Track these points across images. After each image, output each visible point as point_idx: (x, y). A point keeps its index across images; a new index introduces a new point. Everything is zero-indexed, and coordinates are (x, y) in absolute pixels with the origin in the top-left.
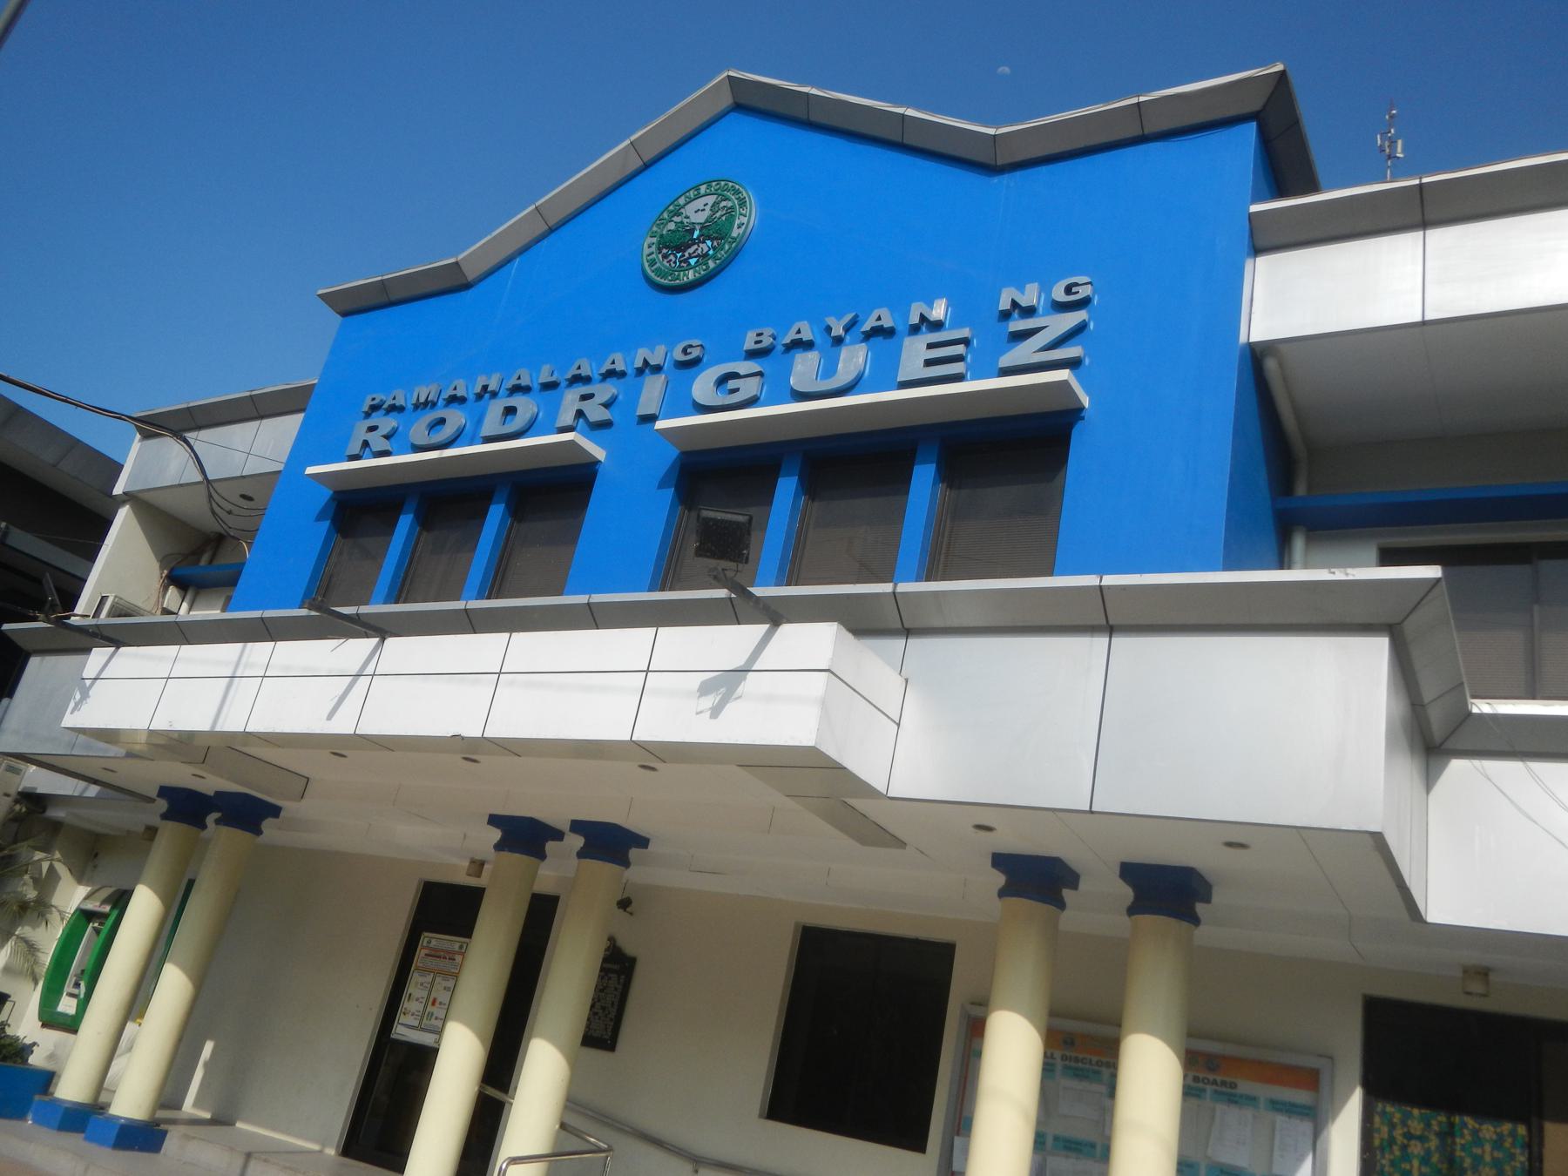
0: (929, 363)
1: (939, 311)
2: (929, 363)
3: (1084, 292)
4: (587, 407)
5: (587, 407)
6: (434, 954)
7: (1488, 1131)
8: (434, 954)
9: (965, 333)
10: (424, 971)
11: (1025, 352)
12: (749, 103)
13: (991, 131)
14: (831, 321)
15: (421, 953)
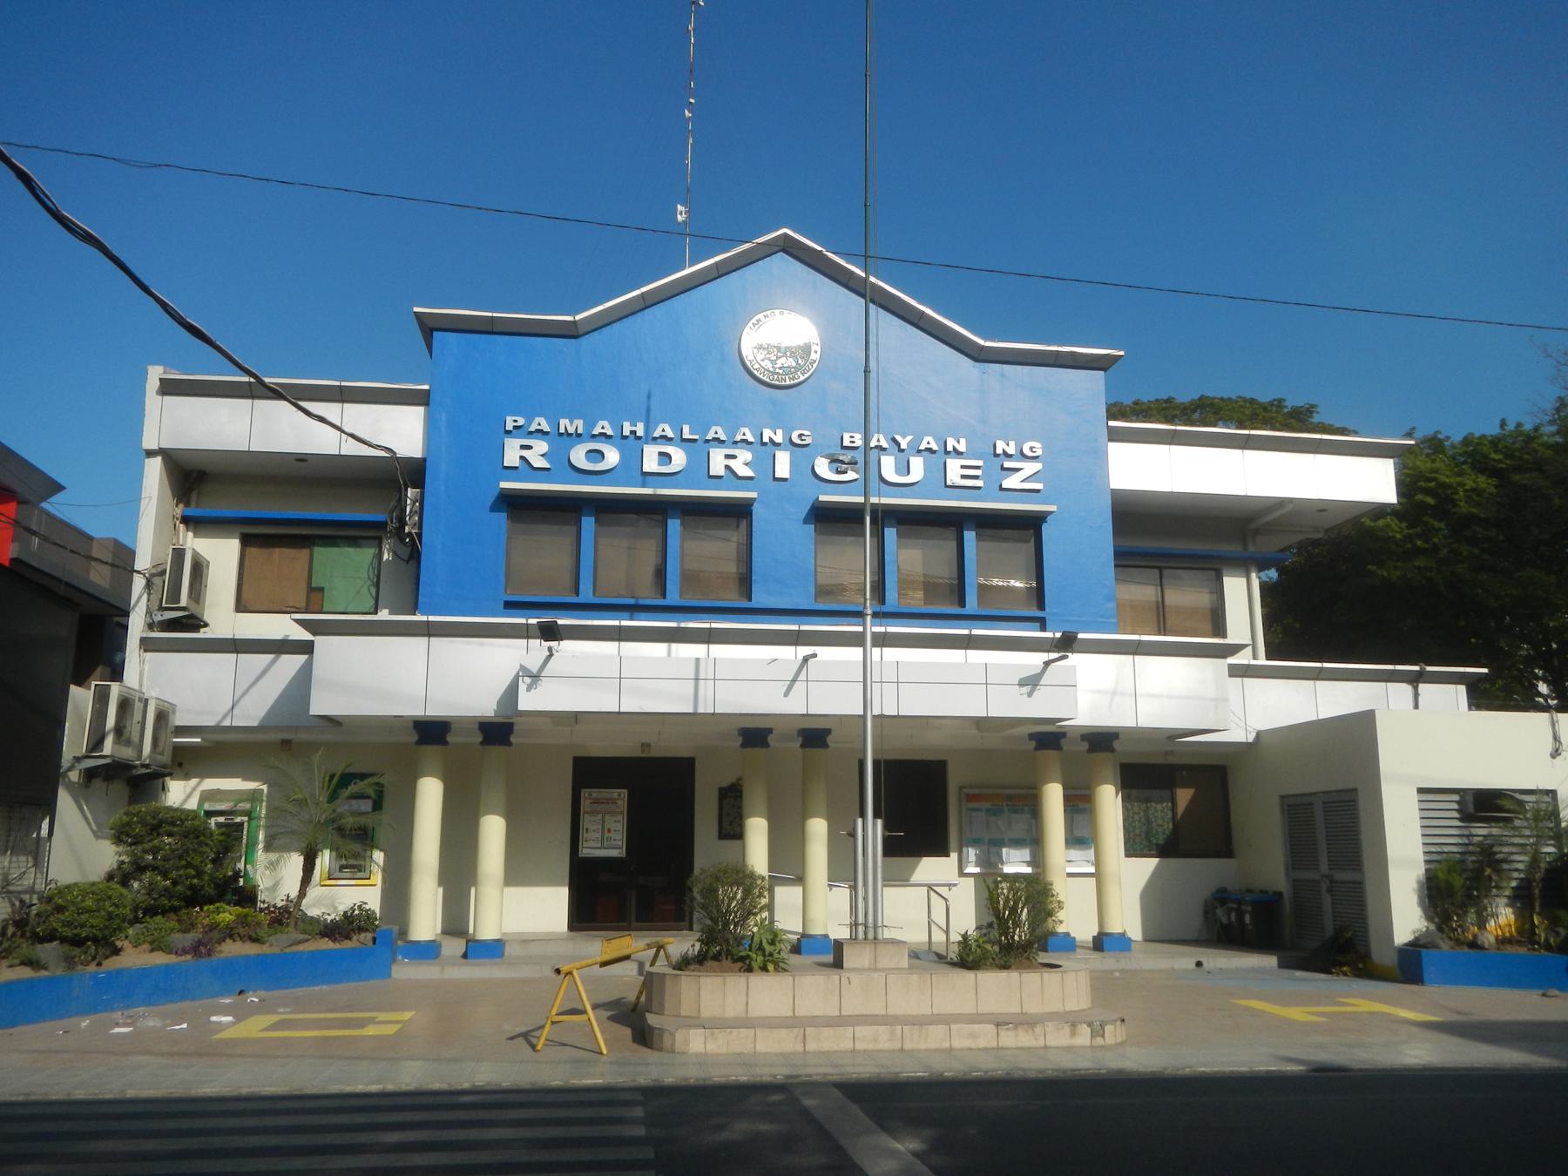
0: (963, 477)
1: (962, 447)
2: (963, 477)
3: (1039, 452)
4: (731, 463)
5: (731, 463)
6: (597, 802)
7: (1159, 807)
8: (597, 802)
9: (979, 463)
10: (593, 813)
11: (1012, 482)
12: (789, 248)
13: (981, 342)
14: (898, 438)
15: (585, 804)
